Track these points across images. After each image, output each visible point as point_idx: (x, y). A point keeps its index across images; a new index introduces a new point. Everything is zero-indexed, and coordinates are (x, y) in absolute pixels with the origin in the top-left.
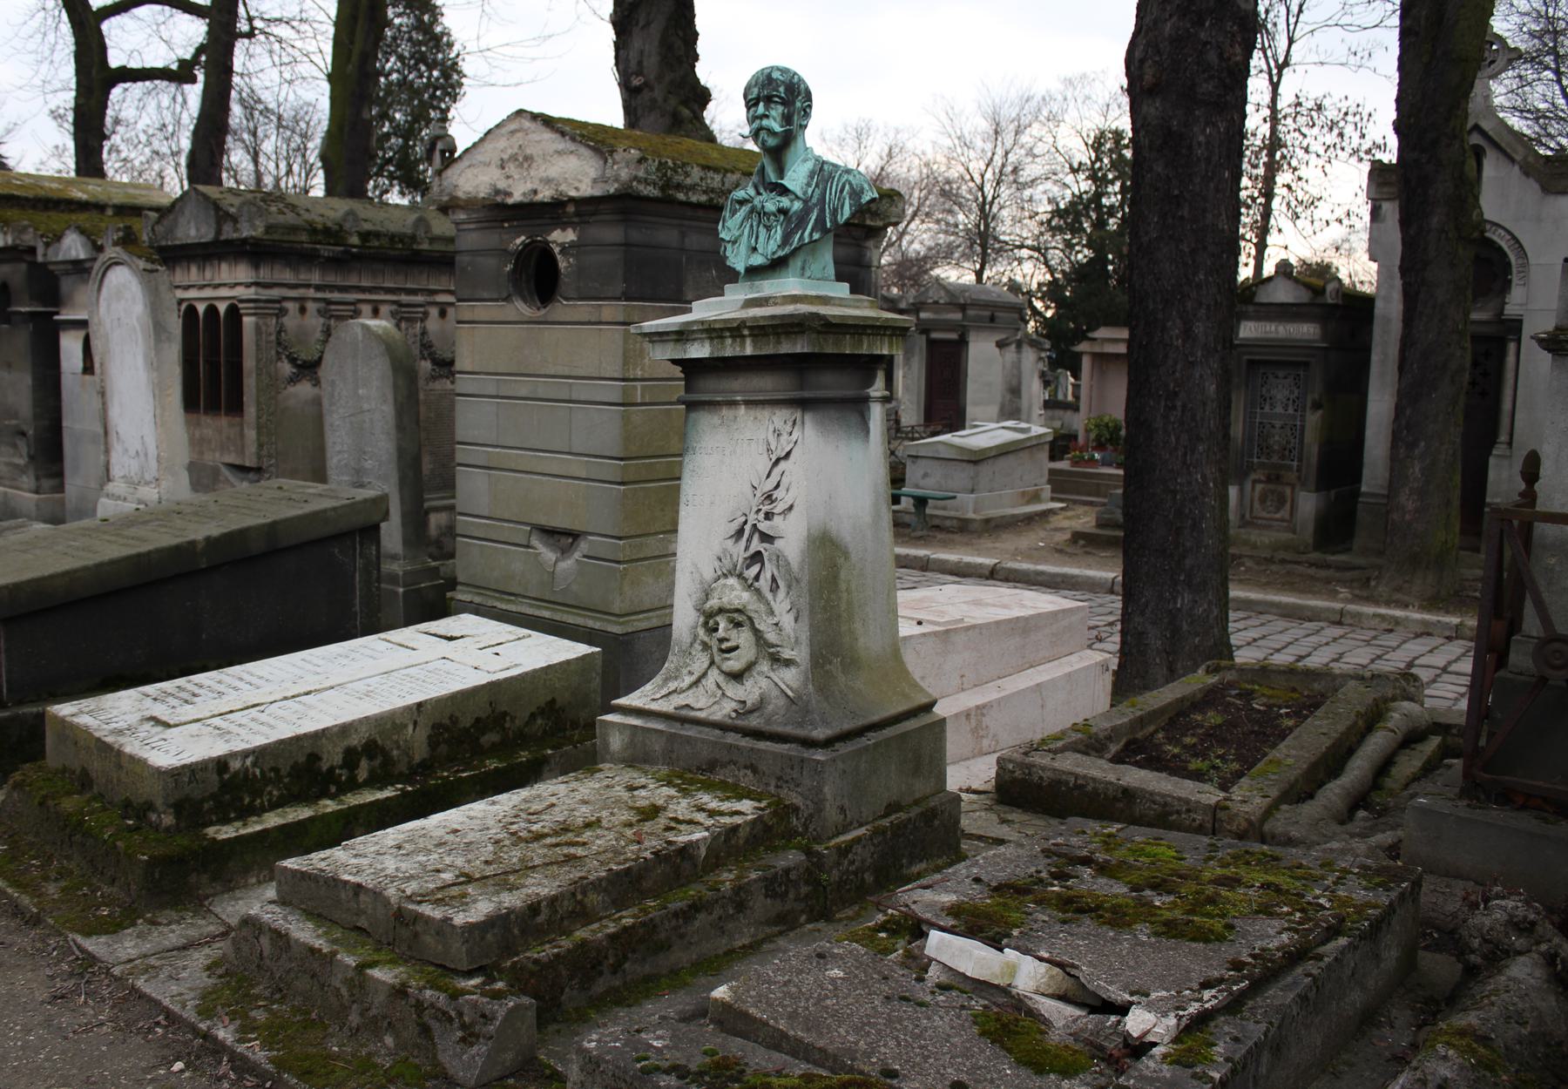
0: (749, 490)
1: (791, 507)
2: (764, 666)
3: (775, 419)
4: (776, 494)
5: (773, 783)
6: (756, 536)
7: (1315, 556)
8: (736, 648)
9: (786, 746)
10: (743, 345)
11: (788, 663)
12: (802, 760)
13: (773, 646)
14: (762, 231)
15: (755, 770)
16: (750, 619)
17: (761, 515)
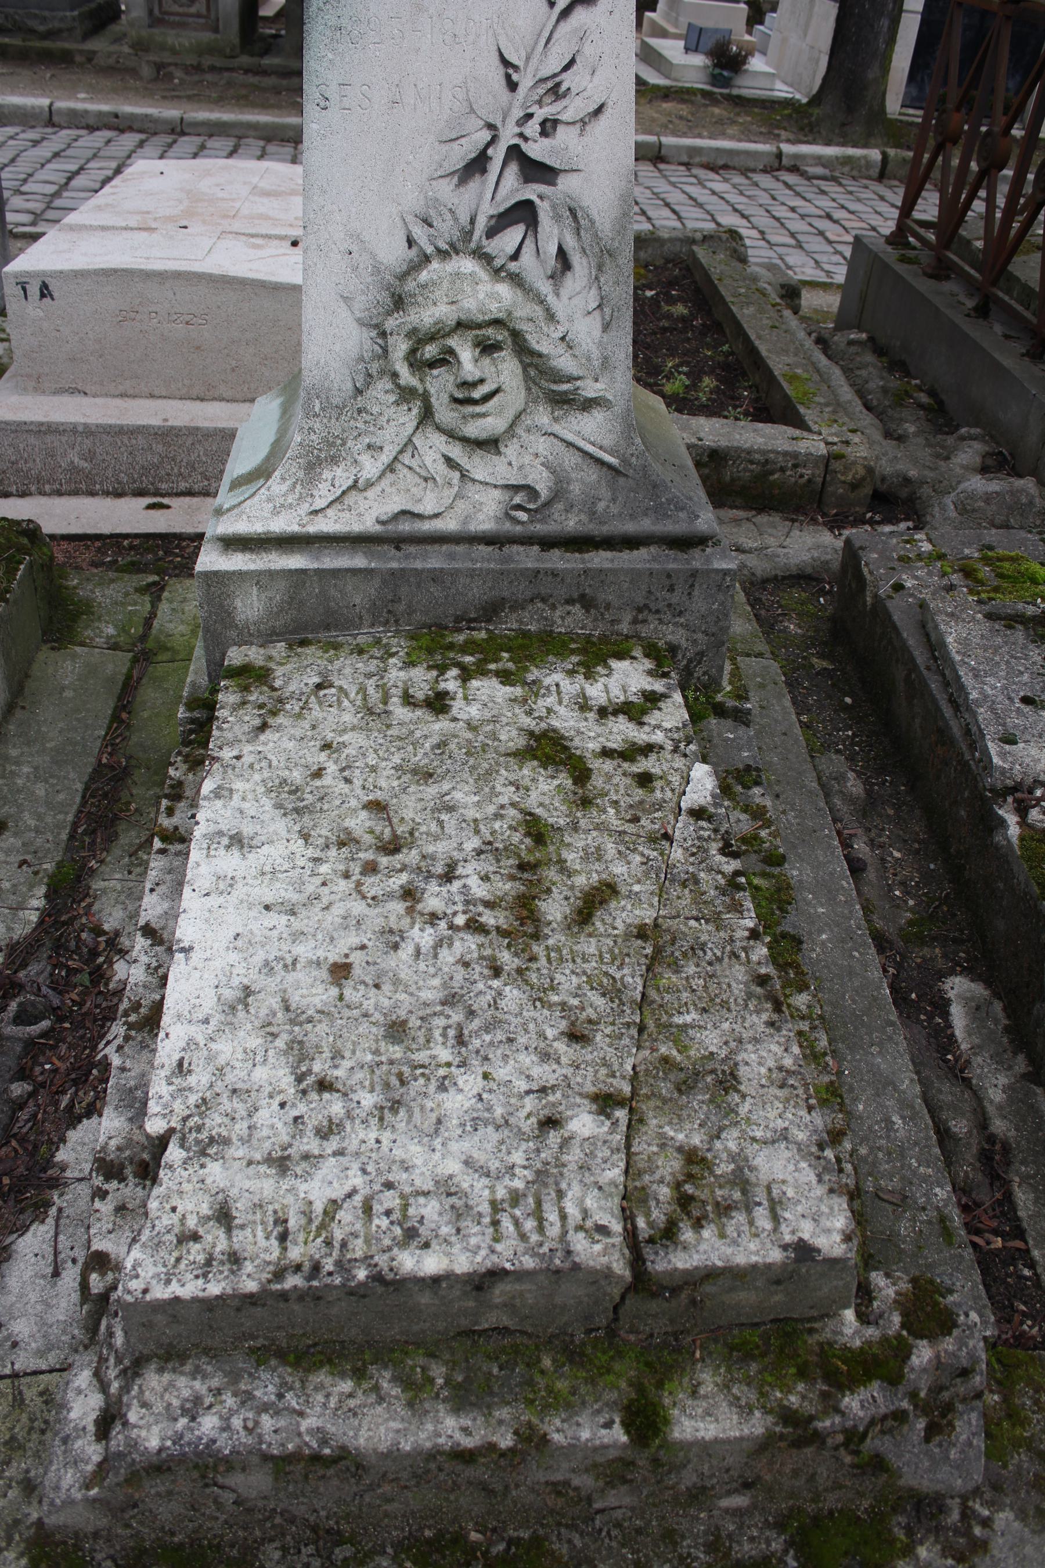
0: (496, 75)
1: (599, 111)
2: (542, 416)
4: (568, 80)
5: (628, 617)
6: (513, 168)
7: (245, 60)
9: (643, 552)
11: (588, 405)
12: (694, 574)
13: (570, 379)
15: (587, 602)
16: (516, 335)
17: (532, 128)
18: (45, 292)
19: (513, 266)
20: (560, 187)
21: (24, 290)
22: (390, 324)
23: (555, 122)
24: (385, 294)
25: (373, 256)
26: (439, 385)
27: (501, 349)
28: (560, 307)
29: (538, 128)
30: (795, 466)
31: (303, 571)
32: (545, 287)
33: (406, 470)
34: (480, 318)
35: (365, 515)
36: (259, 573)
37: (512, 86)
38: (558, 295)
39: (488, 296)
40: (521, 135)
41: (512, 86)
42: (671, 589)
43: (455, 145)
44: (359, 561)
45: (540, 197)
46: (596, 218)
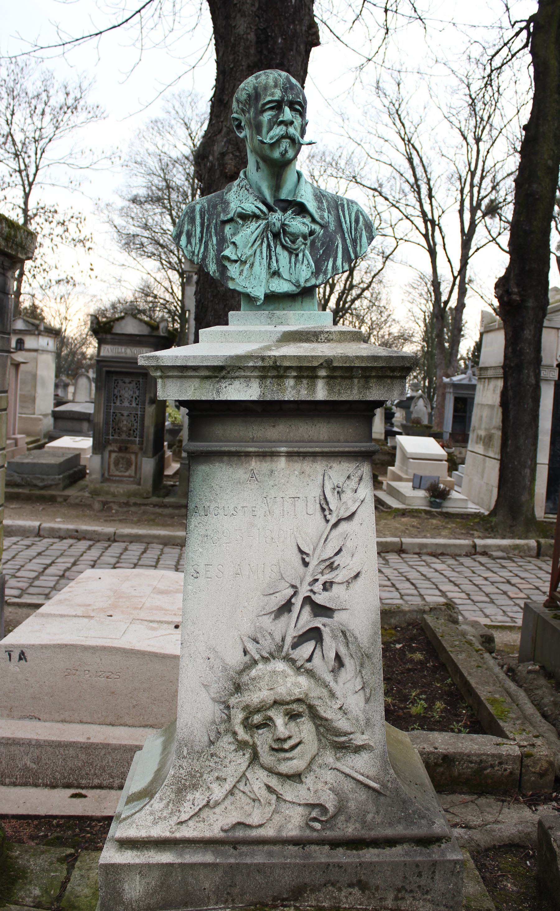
0: (296, 558)
1: (357, 576)
2: (329, 758)
3: (331, 473)
4: (338, 560)
5: (391, 896)
7: (155, 499)
8: (300, 743)
9: (398, 849)
10: (312, 388)
11: (358, 749)
12: (434, 864)
13: (346, 734)
14: (283, 256)
15: (363, 886)
16: (311, 708)
17: (318, 587)
18: (22, 656)
19: (308, 665)
20: (336, 619)
21: (10, 655)
22: (233, 701)
23: (332, 583)
24: (230, 683)
25: (223, 660)
26: (263, 739)
27: (302, 716)
28: (337, 689)
29: (321, 587)
30: (500, 763)
31: (171, 865)
32: (329, 678)
33: (241, 794)
34: (288, 698)
35: (214, 826)
36: (142, 866)
37: (306, 564)
38: (336, 682)
39: (294, 685)
40: (311, 591)
41: (306, 564)
42: (420, 875)
43: (272, 597)
44: (209, 858)
45: (324, 625)
46: (358, 636)
